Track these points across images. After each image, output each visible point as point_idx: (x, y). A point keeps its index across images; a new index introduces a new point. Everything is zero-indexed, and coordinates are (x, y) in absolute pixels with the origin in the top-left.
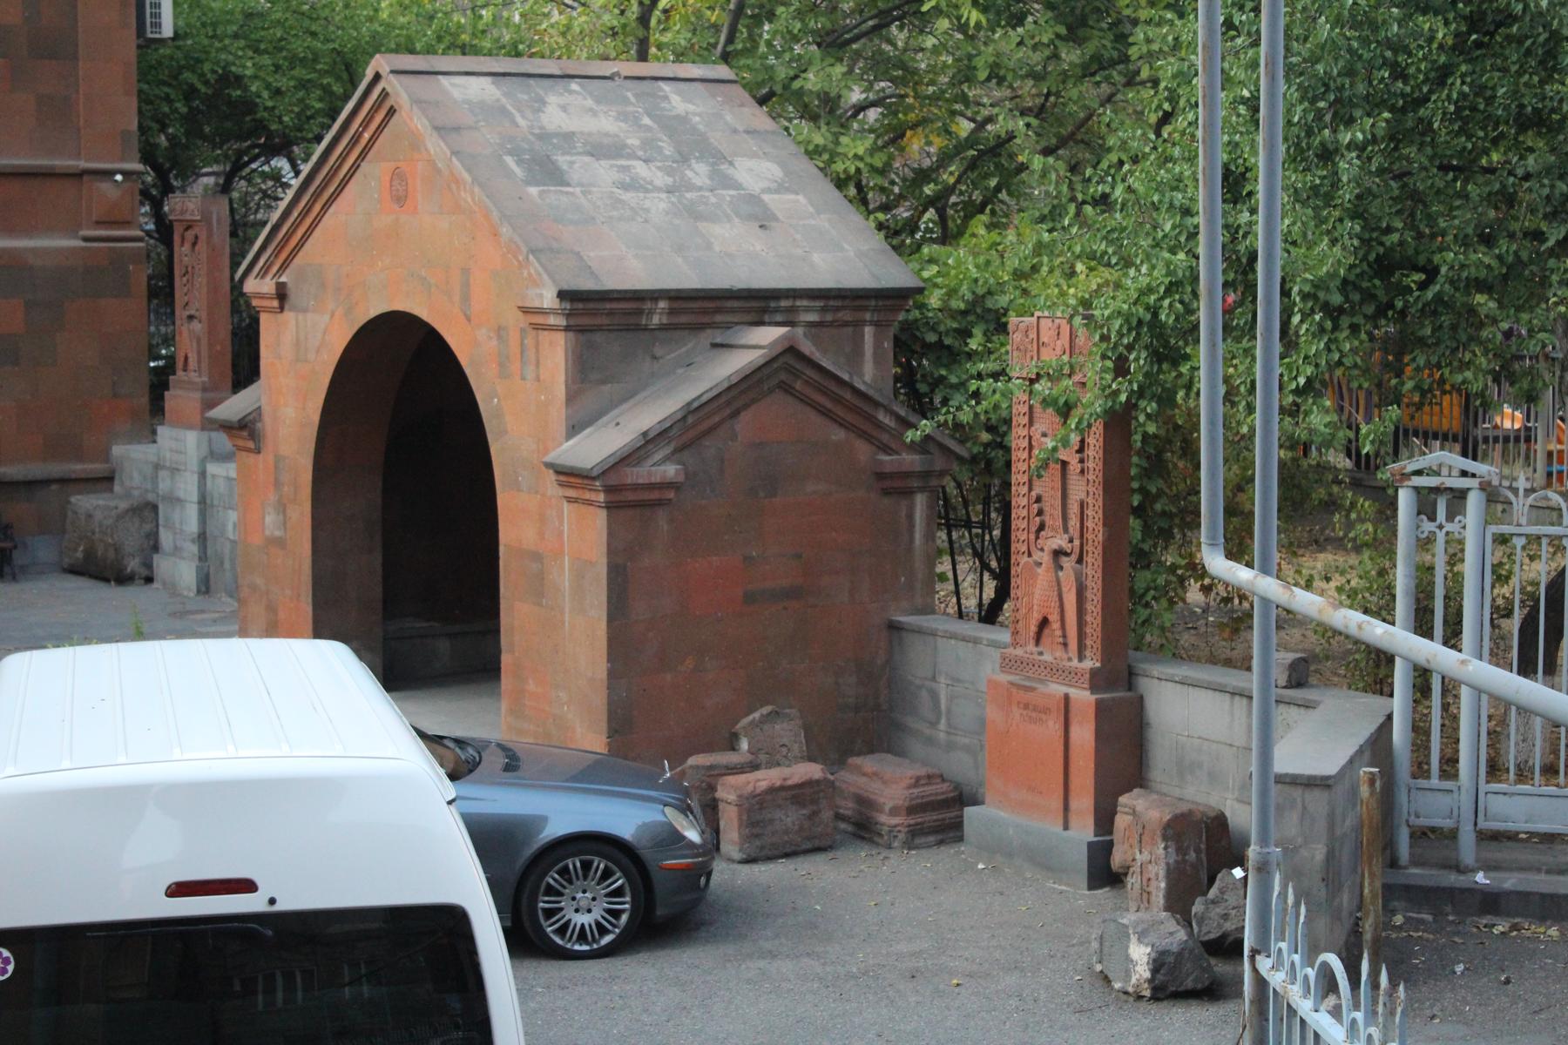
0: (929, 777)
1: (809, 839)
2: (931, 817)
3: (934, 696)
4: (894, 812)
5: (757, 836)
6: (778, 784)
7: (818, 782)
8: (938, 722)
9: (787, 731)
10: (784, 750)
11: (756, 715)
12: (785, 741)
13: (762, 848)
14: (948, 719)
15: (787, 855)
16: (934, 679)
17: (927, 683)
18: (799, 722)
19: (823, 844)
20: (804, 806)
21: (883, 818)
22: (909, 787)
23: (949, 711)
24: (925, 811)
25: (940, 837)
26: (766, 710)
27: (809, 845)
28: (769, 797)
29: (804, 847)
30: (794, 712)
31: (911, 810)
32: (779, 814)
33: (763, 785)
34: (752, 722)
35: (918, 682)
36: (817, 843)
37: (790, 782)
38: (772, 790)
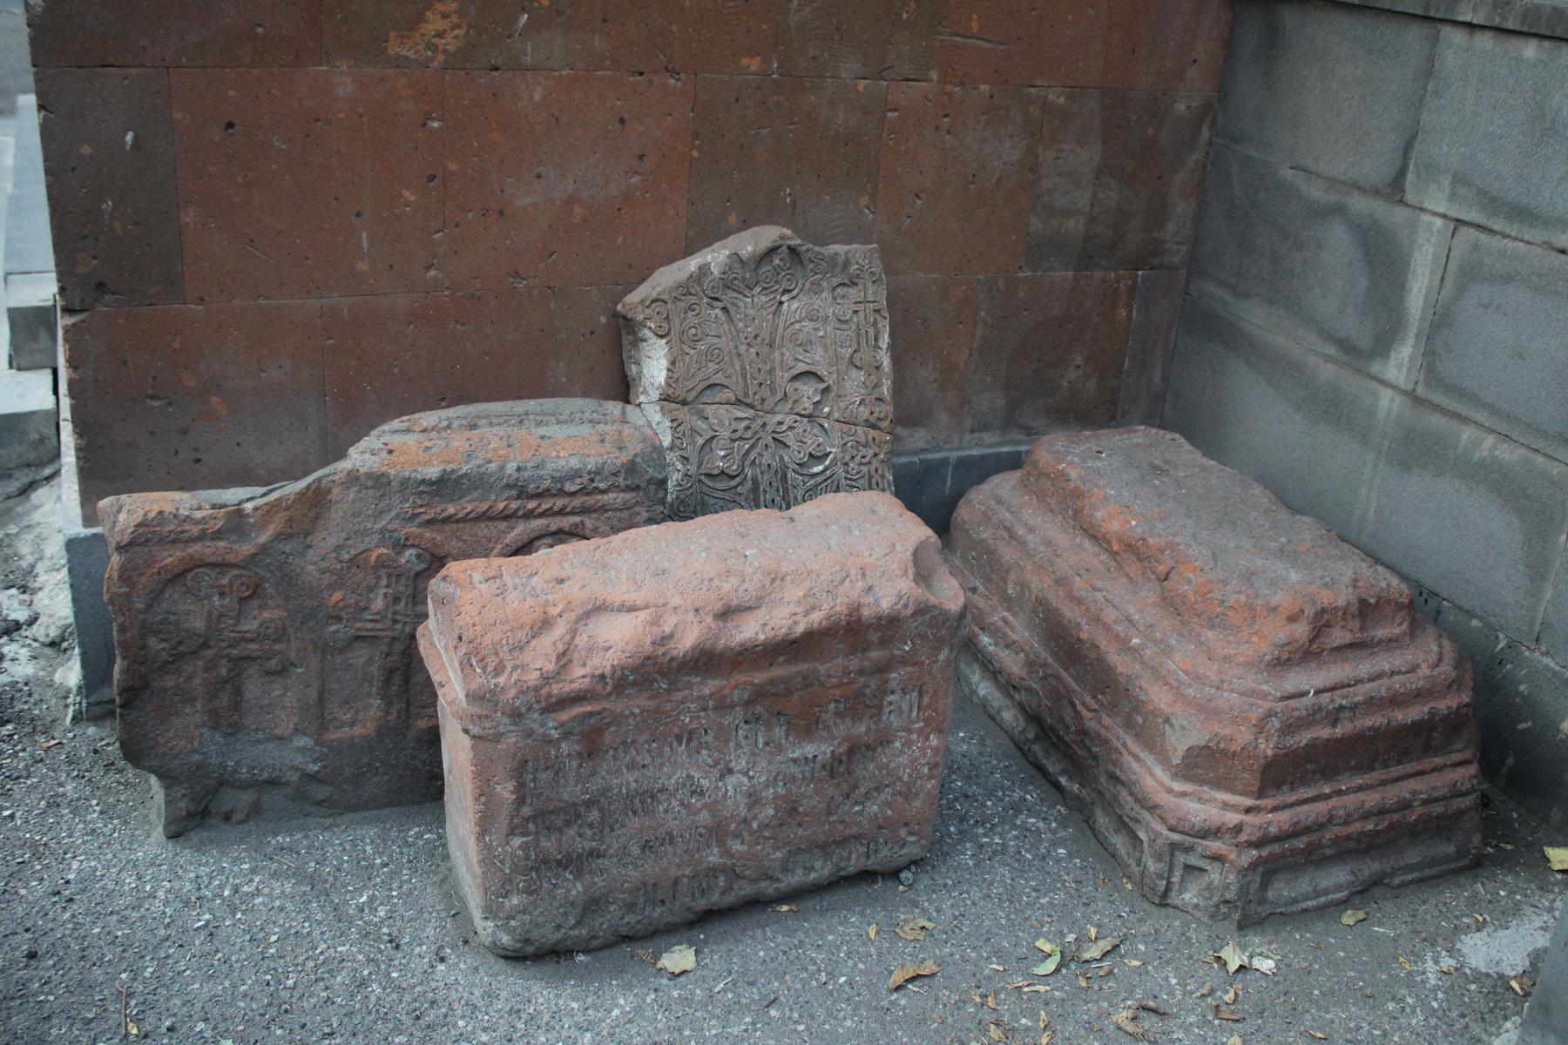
0: (1366, 610)
1: (824, 848)
2: (1351, 799)
3: (1383, 259)
4: (1205, 765)
5: (574, 863)
6: (687, 640)
7: (890, 625)
8: (1383, 344)
9: (831, 337)
10: (809, 390)
11: (715, 257)
12: (817, 358)
13: (593, 905)
14: (1430, 355)
15: (702, 921)
16: (1394, 189)
17: (1360, 204)
18: (878, 294)
19: (884, 856)
20: (806, 726)
21: (1153, 776)
22: (1282, 662)
23: (1440, 321)
24: (1329, 773)
25: (1370, 867)
26: (752, 241)
27: (822, 869)
28: (635, 703)
29: (797, 878)
30: (859, 253)
31: (1279, 774)
32: (679, 769)
33: (617, 639)
34: (685, 289)
35: (1317, 193)
36: (855, 861)
37: (749, 630)
38: (654, 673)
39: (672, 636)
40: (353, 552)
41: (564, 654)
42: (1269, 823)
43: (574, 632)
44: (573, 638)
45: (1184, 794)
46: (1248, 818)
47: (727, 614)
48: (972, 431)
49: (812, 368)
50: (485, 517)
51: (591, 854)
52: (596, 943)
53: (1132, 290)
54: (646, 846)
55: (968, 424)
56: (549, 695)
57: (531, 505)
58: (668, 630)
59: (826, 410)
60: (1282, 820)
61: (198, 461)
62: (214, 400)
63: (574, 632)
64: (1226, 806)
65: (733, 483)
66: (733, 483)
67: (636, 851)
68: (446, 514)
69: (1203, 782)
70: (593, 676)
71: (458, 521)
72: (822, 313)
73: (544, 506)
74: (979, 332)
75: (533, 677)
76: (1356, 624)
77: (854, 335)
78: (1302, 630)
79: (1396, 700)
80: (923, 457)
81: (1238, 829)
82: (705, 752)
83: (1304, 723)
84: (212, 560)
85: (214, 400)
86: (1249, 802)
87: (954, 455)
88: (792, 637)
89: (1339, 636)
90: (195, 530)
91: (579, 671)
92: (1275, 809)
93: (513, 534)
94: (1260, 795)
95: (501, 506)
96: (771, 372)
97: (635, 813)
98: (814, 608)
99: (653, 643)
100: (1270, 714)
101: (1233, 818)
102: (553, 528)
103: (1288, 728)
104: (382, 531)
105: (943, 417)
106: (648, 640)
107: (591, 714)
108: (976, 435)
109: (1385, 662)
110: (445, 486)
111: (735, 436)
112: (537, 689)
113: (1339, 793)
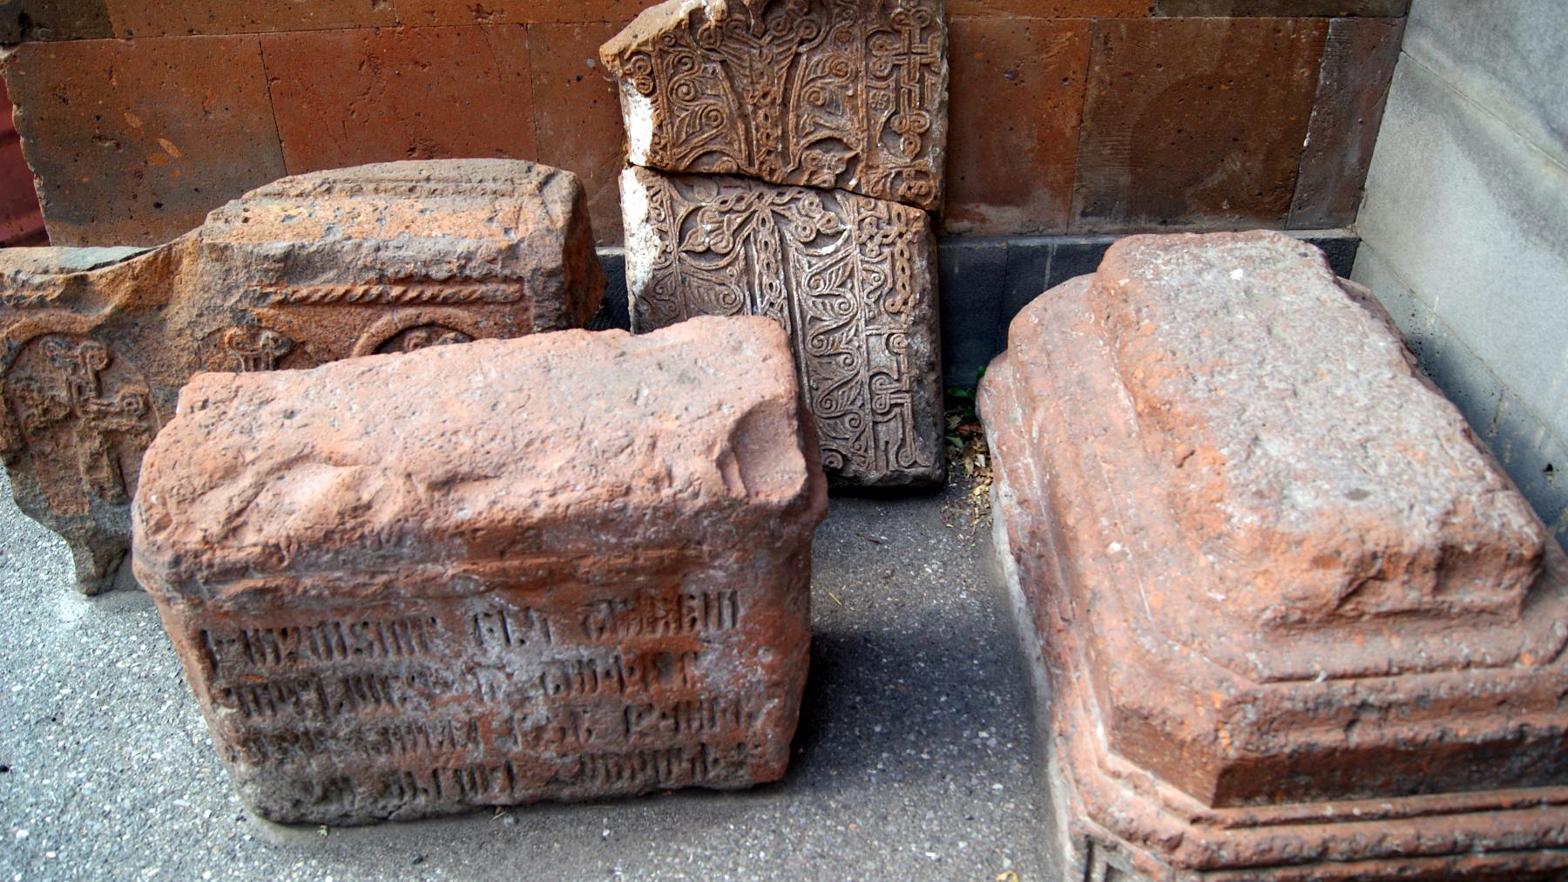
13: (336, 786)
22: (1288, 625)
31: (1241, 782)
39: (368, 506)
40: (207, 330)
41: (239, 513)
42: (1221, 846)
43: (259, 486)
44: (256, 495)
45: (1116, 775)
46: (1193, 831)
47: (449, 482)
48: (1084, 214)
49: (836, 134)
50: (342, 301)
51: (320, 733)
53: (1319, 43)
55: (1079, 206)
56: (210, 566)
57: (396, 291)
58: (366, 497)
59: (853, 182)
60: (1247, 842)
61: (158, 205)
62: (164, 143)
63: (259, 486)
64: (1167, 805)
65: (723, 263)
66: (723, 263)
67: (372, 737)
68: (298, 295)
69: (1145, 765)
71: (315, 304)
72: (852, 67)
73: (412, 294)
74: (1093, 92)
75: (193, 539)
76: (1429, 580)
77: (892, 95)
78: (1333, 581)
79: (1463, 705)
80: (1012, 242)
81: (1174, 844)
83: (1294, 719)
84: (58, 328)
85: (164, 143)
86: (1202, 809)
87: (1055, 243)
88: (525, 523)
89: (1394, 594)
90: (35, 296)
91: (250, 537)
92: (1237, 826)
93: (379, 323)
94: (1219, 801)
95: (359, 290)
96: (784, 137)
98: (564, 487)
99: (341, 514)
100: (1241, 701)
101: (1174, 825)
102: (424, 319)
103: (1265, 725)
104: (232, 309)
105: (1042, 194)
106: (336, 509)
107: (262, 592)
108: (1091, 219)
109: (1461, 644)
110: (292, 265)
111: (725, 208)
112: (197, 555)
113: (1349, 818)
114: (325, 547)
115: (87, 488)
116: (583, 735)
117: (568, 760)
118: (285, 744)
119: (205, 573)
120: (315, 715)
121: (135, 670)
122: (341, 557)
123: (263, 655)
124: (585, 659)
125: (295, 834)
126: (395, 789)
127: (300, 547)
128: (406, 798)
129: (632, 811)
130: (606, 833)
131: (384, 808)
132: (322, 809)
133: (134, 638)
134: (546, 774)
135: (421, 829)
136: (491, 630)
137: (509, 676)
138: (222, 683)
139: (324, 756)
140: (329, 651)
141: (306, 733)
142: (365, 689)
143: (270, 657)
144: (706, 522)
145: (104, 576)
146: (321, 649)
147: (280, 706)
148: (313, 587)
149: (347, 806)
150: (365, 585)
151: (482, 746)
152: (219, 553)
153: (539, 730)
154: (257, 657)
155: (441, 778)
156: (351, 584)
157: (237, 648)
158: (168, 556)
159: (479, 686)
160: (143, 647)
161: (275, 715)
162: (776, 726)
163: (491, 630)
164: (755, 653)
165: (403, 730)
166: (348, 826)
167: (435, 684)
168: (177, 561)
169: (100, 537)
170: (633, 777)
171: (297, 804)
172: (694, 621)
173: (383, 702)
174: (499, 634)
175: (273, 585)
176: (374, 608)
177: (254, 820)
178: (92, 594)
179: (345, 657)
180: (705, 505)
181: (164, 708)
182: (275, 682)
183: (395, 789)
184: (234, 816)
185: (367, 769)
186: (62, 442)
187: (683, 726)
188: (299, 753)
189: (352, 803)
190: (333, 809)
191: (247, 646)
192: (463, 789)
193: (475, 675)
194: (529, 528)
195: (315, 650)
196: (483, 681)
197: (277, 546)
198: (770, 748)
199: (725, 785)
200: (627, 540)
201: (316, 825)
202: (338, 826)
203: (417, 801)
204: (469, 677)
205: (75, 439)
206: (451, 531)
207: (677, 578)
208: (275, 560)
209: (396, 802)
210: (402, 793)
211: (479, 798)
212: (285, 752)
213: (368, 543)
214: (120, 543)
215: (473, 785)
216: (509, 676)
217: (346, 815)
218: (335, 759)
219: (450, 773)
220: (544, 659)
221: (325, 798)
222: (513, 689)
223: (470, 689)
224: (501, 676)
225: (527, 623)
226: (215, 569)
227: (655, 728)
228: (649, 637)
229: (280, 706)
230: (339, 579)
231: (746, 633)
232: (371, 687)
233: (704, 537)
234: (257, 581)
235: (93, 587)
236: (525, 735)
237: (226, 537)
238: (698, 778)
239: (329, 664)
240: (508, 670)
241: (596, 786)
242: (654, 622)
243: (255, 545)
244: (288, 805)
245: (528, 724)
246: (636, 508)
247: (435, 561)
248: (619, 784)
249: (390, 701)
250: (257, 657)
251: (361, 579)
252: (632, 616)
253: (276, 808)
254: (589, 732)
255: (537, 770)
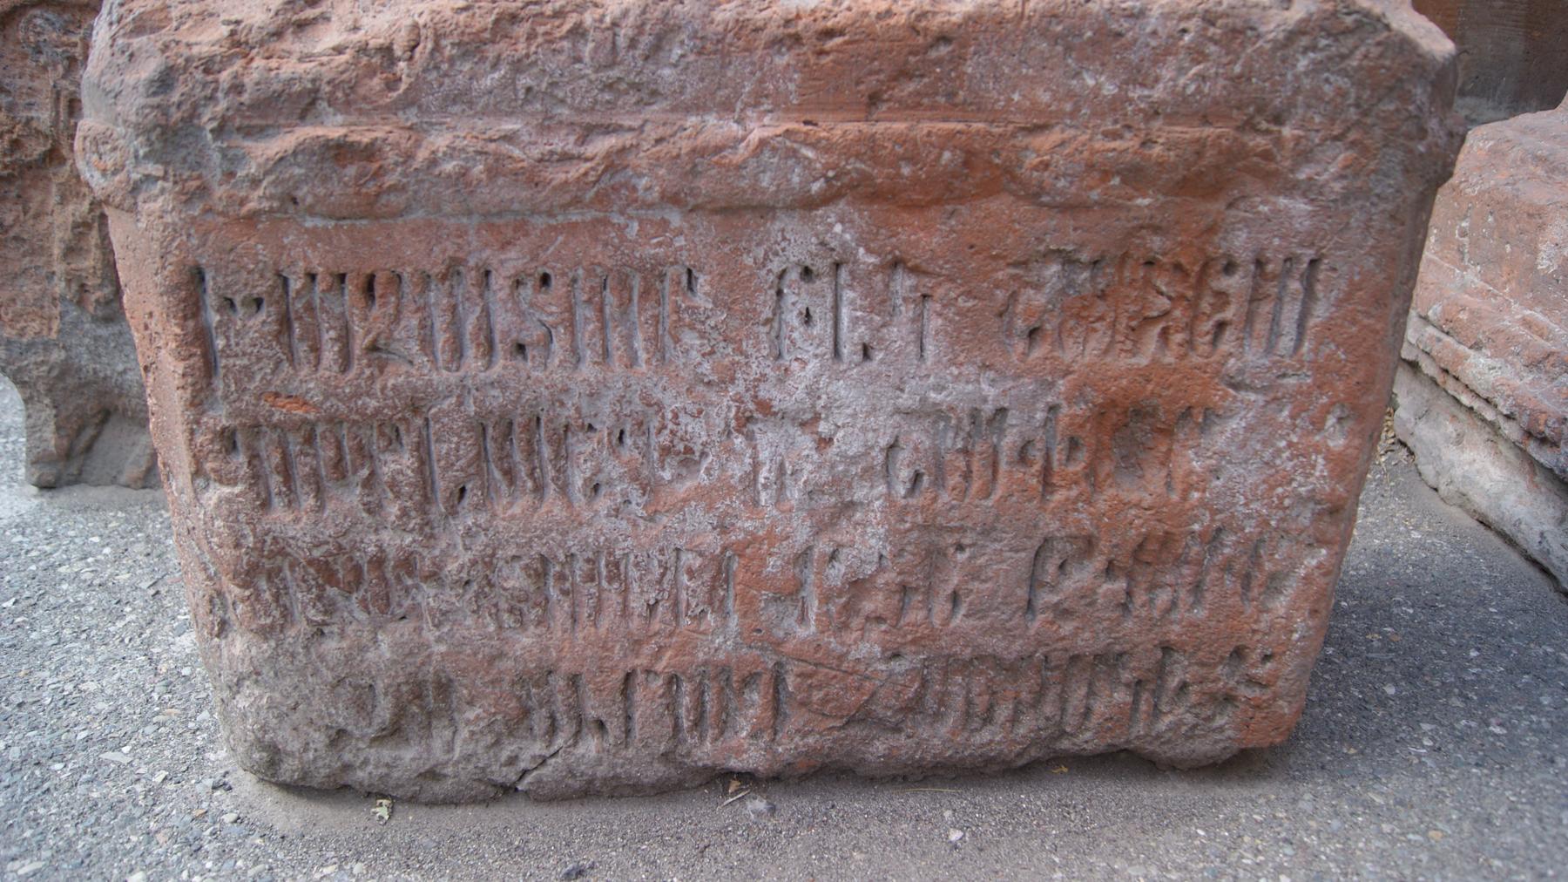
13: (424, 700)
51: (407, 563)
52: (439, 789)
54: (540, 570)
56: (237, 88)
67: (515, 579)
70: (363, 49)
82: (690, 339)
88: (935, 23)
91: (329, 37)
97: (510, 475)
107: (340, 151)
112: (209, 66)
114: (491, 52)
115: (59, 287)
116: (940, 606)
117: (899, 666)
118: (331, 591)
119: (223, 105)
120: (404, 513)
121: (87, 576)
122: (524, 81)
123: (316, 349)
124: (988, 409)
125: (328, 817)
126: (539, 721)
127: (437, 48)
128: (559, 741)
129: (998, 800)
130: (955, 835)
131: (512, 761)
132: (387, 754)
133: (96, 539)
134: (852, 699)
135: (578, 815)
136: (807, 318)
137: (824, 442)
138: (220, 417)
139: (406, 627)
140: (458, 352)
141: (378, 562)
142: (518, 457)
143: (330, 354)
144: (1303, 63)
145: (67, 455)
146: (441, 339)
147: (333, 489)
148: (452, 152)
149: (438, 753)
150: (566, 158)
151: (734, 622)
152: (259, 63)
153: (857, 586)
154: (302, 349)
155: (639, 695)
156: (536, 152)
157: (264, 319)
158: (149, 68)
159: (756, 466)
160: (107, 550)
161: (321, 508)
162: (1314, 612)
163: (807, 318)
164: (1318, 424)
165: (580, 567)
166: (432, 804)
167: (666, 451)
168: (164, 81)
169: (71, 381)
170: (1014, 720)
171: (339, 737)
172: (1221, 326)
173: (551, 489)
174: (821, 327)
175: (366, 139)
176: (572, 228)
177: (247, 784)
178: (46, 487)
179: (489, 366)
180: (1306, 21)
181: (120, 624)
182: (334, 420)
183: (539, 721)
184: (209, 782)
185: (492, 660)
186: (33, 206)
187: (1140, 597)
188: (355, 612)
189: (450, 748)
190: (409, 757)
191: (285, 322)
192: (677, 727)
193: (750, 437)
194: (943, 38)
195: (427, 343)
196: (764, 455)
197: (387, 51)
198: (1289, 665)
199: (1183, 749)
200: (1136, 93)
201: (371, 794)
202: (413, 800)
203: (580, 750)
204: (738, 441)
205: (54, 199)
206: (773, 30)
207: (1218, 206)
208: (376, 82)
209: (538, 748)
210: (553, 729)
211: (705, 751)
212: (330, 609)
213: (587, 49)
214: (102, 394)
215: (698, 723)
216: (824, 442)
217: (433, 775)
218: (430, 635)
219: (658, 684)
220: (905, 400)
221: (393, 732)
222: (825, 476)
223: (737, 470)
224: (806, 443)
225: (881, 305)
226: (245, 98)
227: (1087, 595)
228: (1125, 362)
229: (333, 489)
230: (509, 138)
231: (1318, 368)
232: (531, 452)
233: (1291, 104)
234: (332, 128)
235: (49, 474)
236: (826, 598)
237: (278, 34)
238: (1140, 729)
239: (453, 378)
240: (823, 427)
241: (937, 737)
242: (1136, 331)
243: (339, 50)
244: (319, 739)
245: (837, 573)
246: (1166, 16)
247: (726, 107)
248: (985, 736)
249: (564, 489)
250: (302, 349)
251: (562, 142)
252: (1101, 307)
253: (295, 746)
254: (955, 598)
255: (835, 689)
